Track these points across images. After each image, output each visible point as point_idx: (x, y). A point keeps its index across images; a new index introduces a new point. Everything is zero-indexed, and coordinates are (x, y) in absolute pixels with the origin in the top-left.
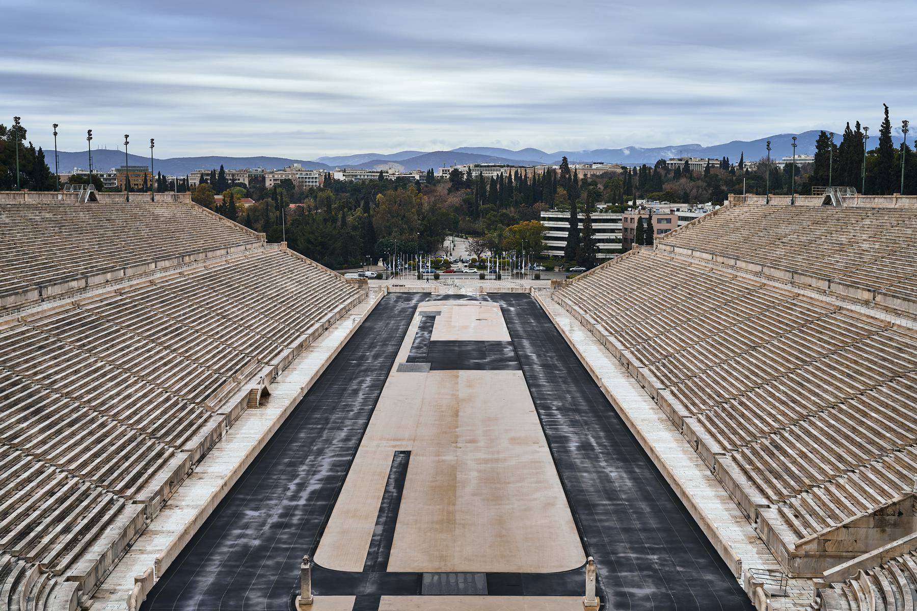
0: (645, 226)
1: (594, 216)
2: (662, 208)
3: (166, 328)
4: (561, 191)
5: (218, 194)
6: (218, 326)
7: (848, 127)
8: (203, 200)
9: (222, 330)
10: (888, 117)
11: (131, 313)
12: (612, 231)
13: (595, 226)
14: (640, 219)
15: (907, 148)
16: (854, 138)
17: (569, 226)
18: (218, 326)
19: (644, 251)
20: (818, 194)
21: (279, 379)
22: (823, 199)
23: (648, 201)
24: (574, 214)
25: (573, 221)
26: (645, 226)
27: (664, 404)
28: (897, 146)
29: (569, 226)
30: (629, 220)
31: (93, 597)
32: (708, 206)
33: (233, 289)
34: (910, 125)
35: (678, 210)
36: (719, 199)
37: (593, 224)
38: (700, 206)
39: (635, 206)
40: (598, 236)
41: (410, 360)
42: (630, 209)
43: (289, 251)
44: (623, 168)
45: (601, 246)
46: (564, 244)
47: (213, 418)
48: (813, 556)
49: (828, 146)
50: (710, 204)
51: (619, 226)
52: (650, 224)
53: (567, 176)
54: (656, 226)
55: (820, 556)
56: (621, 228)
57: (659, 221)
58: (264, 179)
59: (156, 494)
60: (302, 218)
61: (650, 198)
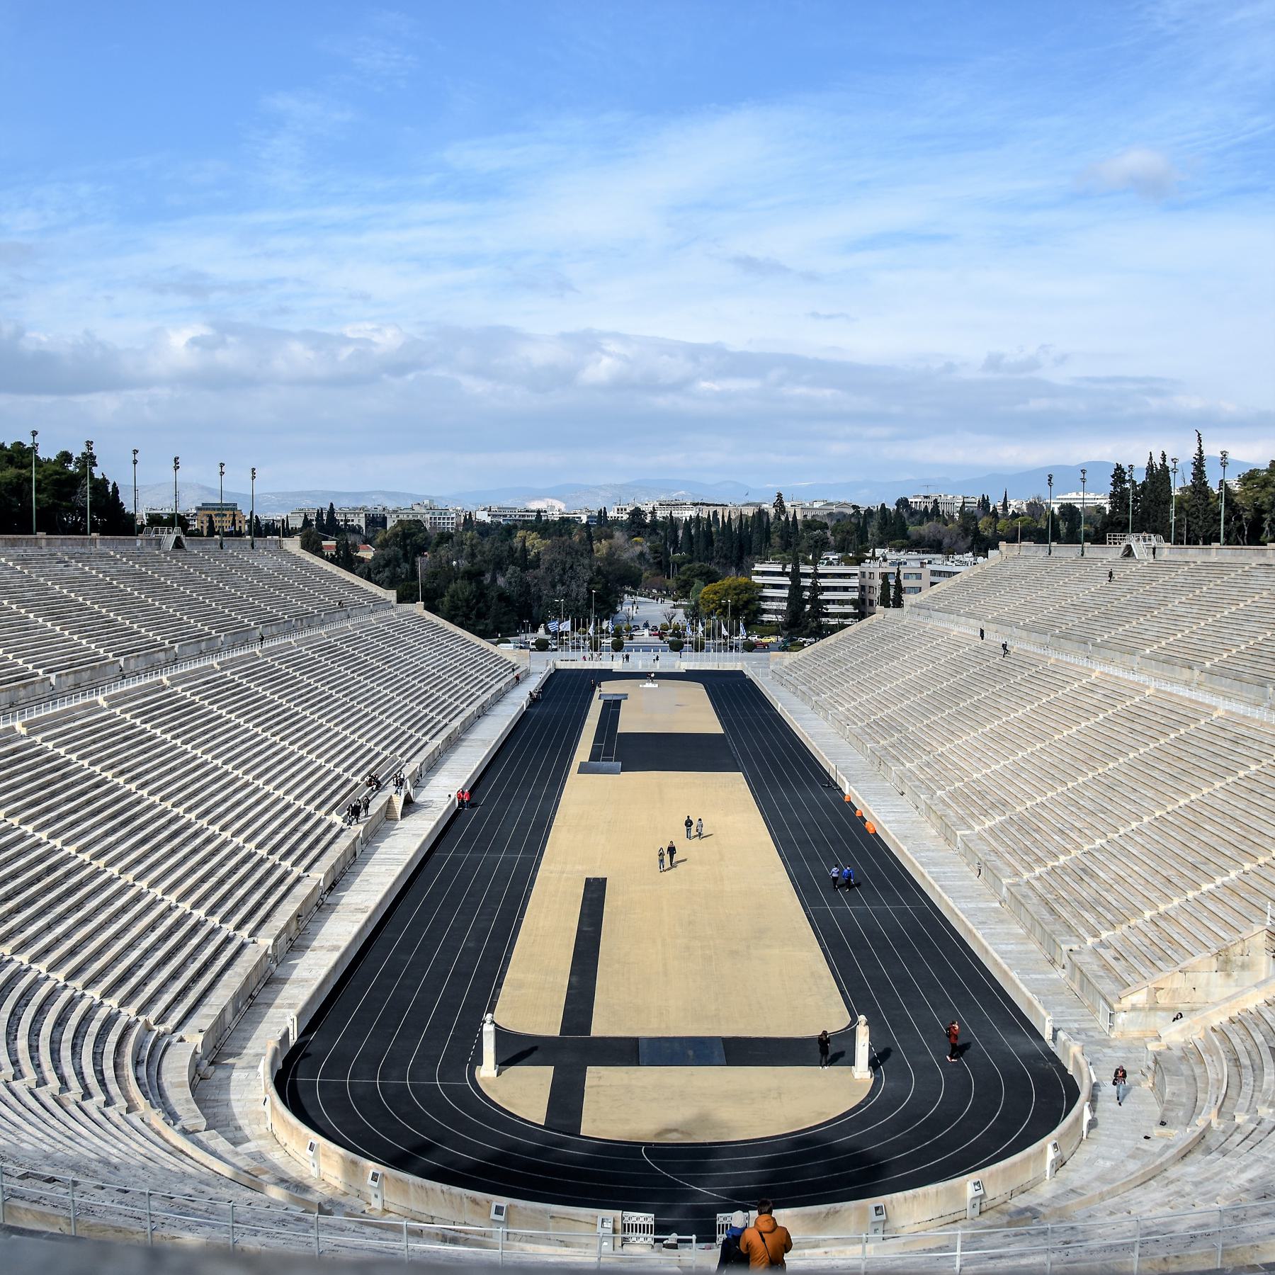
0: (892, 582)
1: (822, 569)
2: (911, 560)
3: (279, 715)
4: (776, 540)
5: (326, 539)
6: (343, 712)
7: (1151, 458)
8: (312, 546)
9: (348, 718)
10: (1201, 446)
11: (234, 695)
12: (846, 589)
13: (823, 582)
14: (885, 577)
15: (1227, 489)
16: (1159, 476)
17: (790, 583)
18: (343, 712)
19: (892, 612)
20: (1115, 543)
21: (423, 781)
22: (1122, 549)
23: (890, 551)
24: (796, 569)
25: (796, 576)
26: (892, 582)
27: (932, 816)
28: (1214, 486)
29: (790, 583)
30: (867, 575)
31: (212, 1063)
32: (969, 557)
33: (359, 664)
34: (1229, 456)
35: (930, 562)
36: (982, 546)
37: (821, 580)
38: (957, 557)
39: (874, 558)
40: (826, 596)
41: (594, 756)
42: (868, 561)
43: (429, 616)
44: (854, 507)
45: (832, 609)
46: (784, 606)
47: (345, 833)
48: (1141, 1010)
49: (1124, 482)
50: (970, 554)
51: (854, 582)
52: (898, 581)
53: (783, 518)
54: (905, 583)
55: (1151, 1009)
56: (858, 585)
57: (907, 576)
58: (385, 519)
59: (282, 932)
60: (443, 575)
61: (894, 546)
